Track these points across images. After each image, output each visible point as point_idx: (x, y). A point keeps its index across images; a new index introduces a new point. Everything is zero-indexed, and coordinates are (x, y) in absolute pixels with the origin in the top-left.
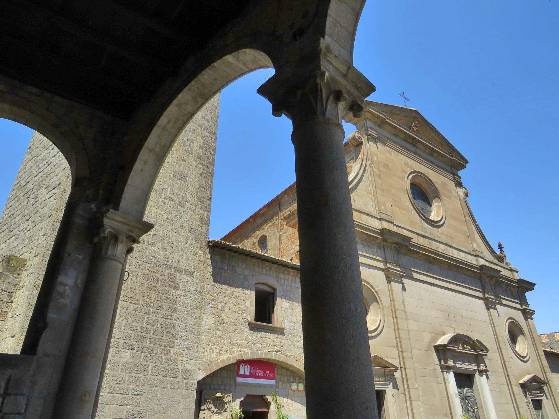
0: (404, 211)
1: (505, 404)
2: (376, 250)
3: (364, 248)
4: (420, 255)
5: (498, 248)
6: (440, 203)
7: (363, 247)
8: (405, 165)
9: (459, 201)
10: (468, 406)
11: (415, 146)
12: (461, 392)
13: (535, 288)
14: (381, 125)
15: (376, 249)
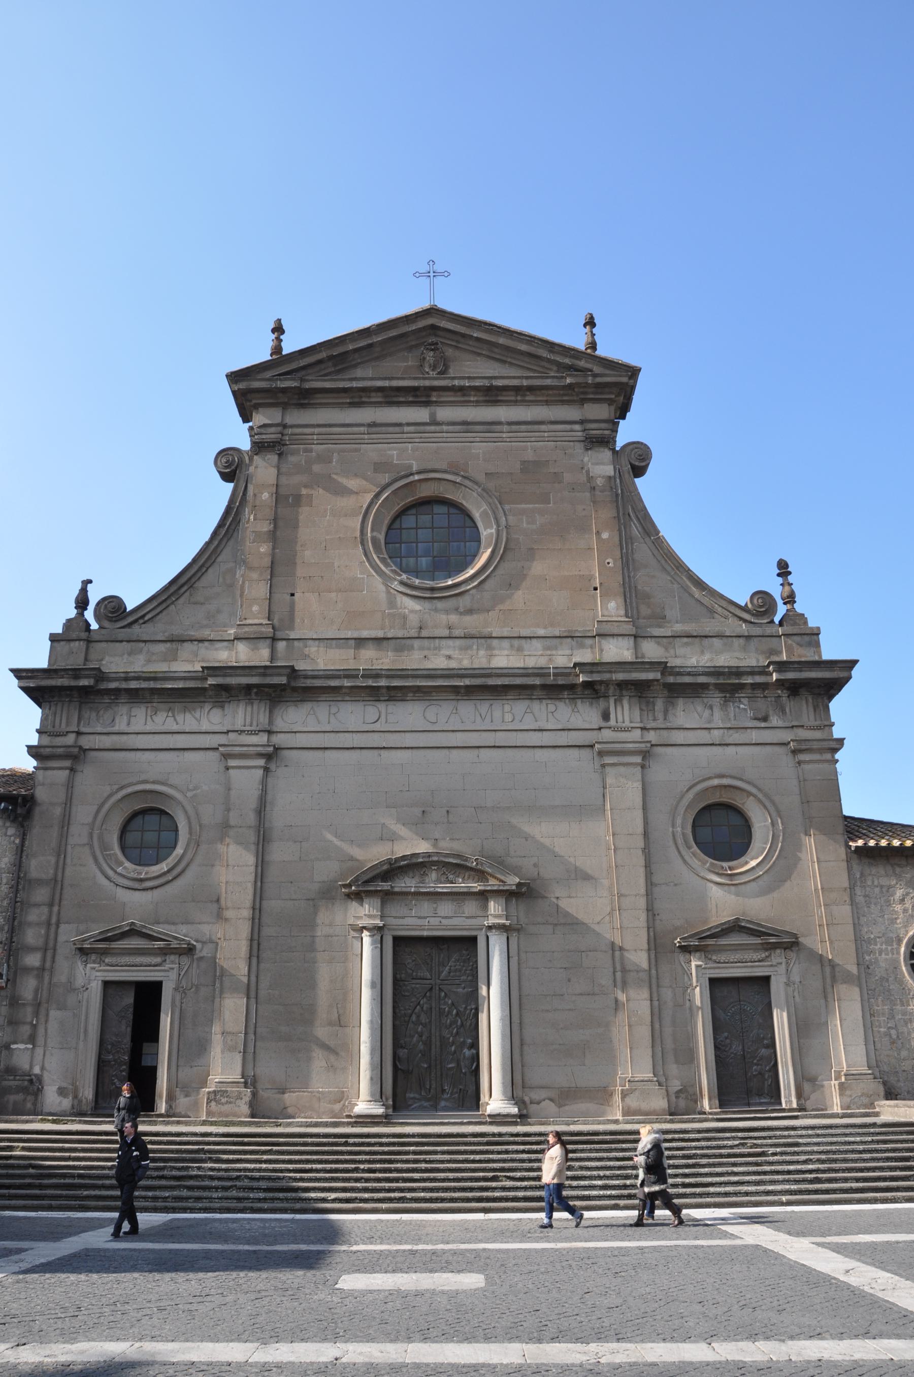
0: (333, 595)
1: (581, 994)
2: (209, 711)
3: (174, 716)
4: (344, 690)
5: (779, 575)
6: (491, 527)
7: (170, 714)
8: (376, 470)
9: (588, 494)
10: (445, 1003)
11: (427, 404)
12: (429, 976)
13: (854, 672)
14: (302, 402)
15: (207, 711)
